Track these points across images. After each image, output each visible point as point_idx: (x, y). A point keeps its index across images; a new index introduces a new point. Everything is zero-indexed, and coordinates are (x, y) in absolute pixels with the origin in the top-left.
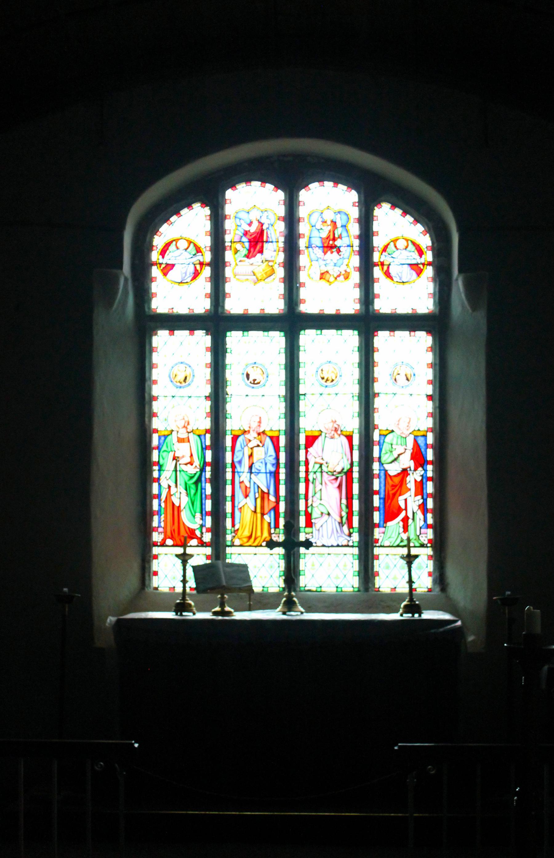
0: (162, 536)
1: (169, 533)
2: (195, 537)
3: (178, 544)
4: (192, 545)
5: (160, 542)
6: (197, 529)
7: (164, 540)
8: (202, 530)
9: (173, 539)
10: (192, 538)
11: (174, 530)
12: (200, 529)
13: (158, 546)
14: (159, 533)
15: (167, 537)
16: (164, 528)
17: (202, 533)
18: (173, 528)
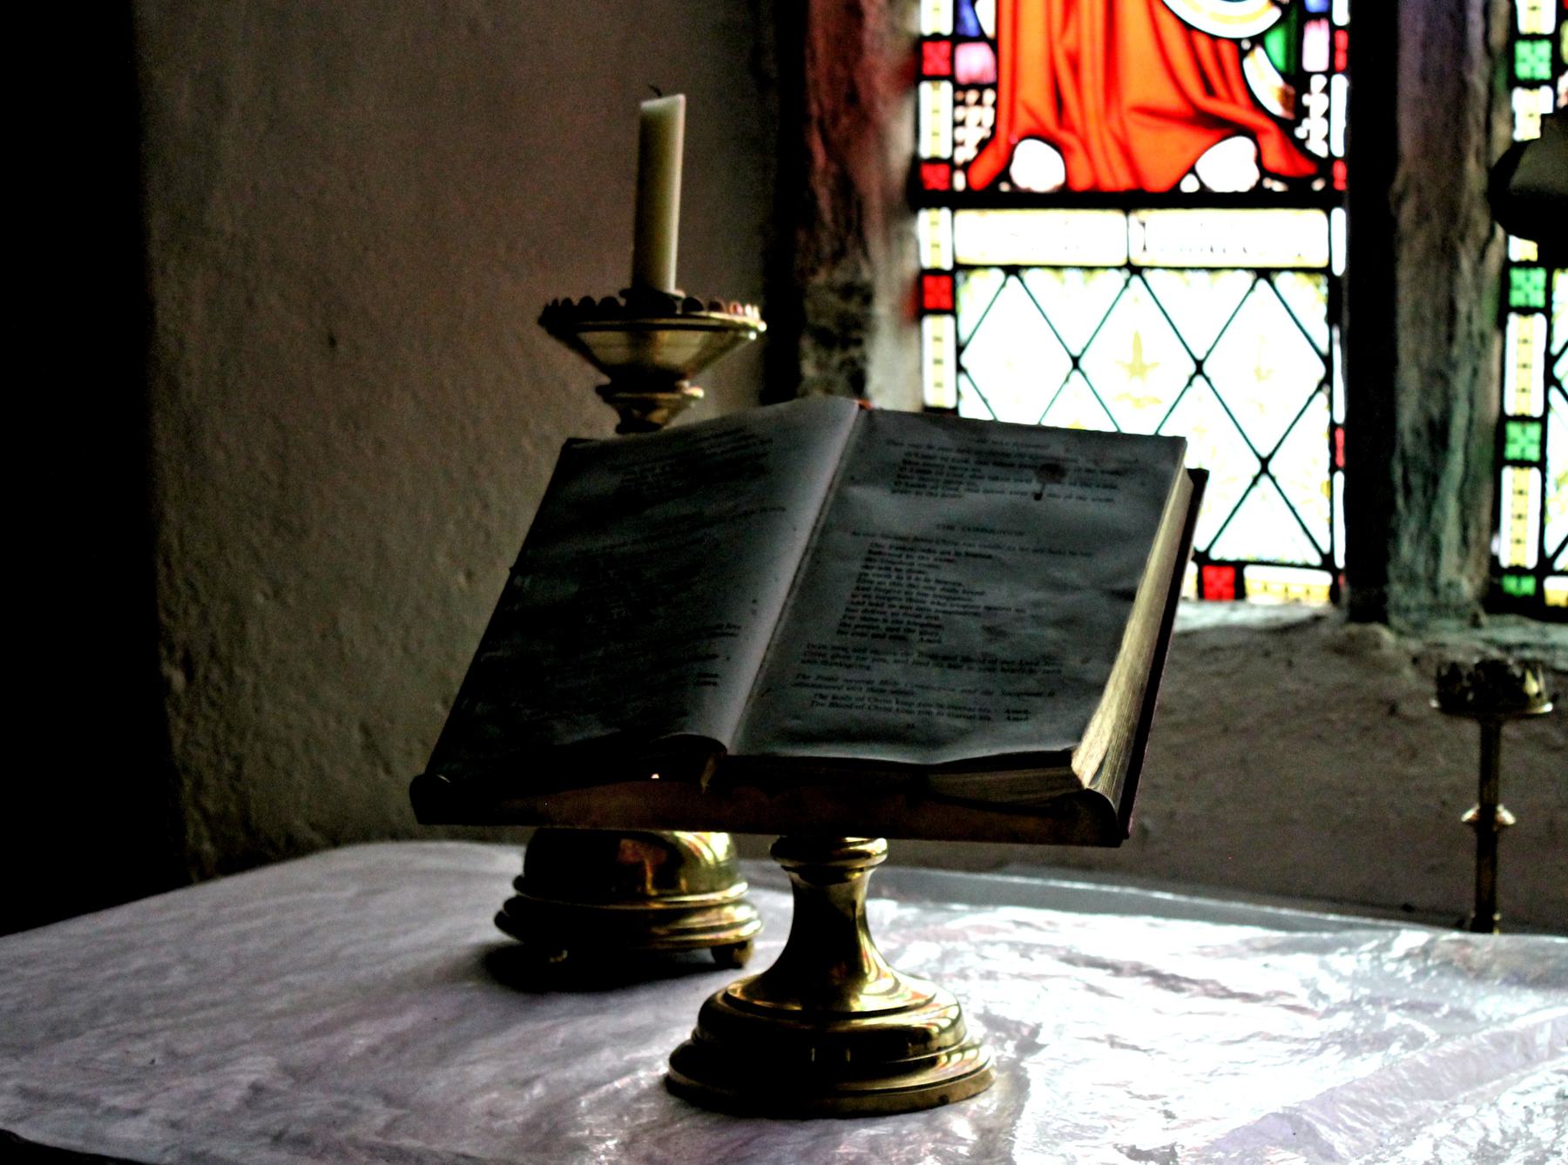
0: (980, 118)
1: (1034, 91)
2: (1242, 114)
3: (1108, 183)
4: (1218, 185)
5: (967, 167)
6: (1259, 40)
7: (997, 146)
8: (1295, 49)
9: (1066, 137)
10: (1225, 128)
11: (1074, 62)
12: (1276, 42)
13: (956, 202)
14: (959, 87)
15: (1024, 121)
16: (994, 44)
17: (1296, 79)
18: (1070, 40)
